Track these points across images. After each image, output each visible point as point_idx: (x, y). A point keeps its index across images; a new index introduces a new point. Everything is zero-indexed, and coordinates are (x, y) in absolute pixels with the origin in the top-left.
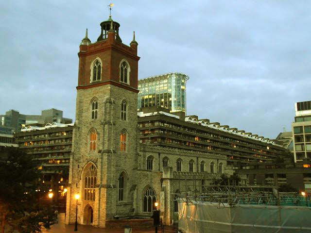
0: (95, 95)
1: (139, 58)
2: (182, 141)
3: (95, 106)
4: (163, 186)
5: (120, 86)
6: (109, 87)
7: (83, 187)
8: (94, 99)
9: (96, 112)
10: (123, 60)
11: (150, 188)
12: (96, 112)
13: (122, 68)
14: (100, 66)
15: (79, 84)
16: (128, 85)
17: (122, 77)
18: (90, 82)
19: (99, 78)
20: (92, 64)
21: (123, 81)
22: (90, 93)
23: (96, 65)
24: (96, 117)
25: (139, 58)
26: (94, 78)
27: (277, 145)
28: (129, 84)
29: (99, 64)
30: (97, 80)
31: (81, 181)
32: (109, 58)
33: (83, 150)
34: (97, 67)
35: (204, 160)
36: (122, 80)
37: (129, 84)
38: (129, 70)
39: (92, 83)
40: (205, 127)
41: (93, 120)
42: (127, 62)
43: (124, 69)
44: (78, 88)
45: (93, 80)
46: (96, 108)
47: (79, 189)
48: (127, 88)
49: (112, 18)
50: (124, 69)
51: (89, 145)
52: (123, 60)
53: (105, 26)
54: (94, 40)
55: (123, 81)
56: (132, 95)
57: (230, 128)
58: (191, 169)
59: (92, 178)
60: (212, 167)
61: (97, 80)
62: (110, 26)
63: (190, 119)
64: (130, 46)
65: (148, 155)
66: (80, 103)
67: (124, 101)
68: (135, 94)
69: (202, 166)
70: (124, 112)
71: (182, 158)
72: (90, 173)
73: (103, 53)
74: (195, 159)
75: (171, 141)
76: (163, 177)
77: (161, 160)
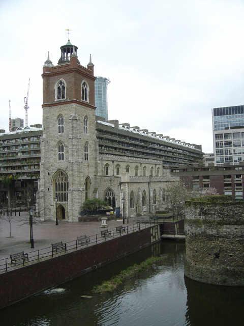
0: (60, 113)
2: (117, 148)
4: (121, 188)
7: (54, 191)
8: (60, 116)
9: (62, 127)
10: (83, 81)
11: (110, 190)
13: (83, 88)
14: (63, 87)
15: (43, 103)
17: (83, 96)
18: (56, 101)
19: (63, 97)
20: (56, 84)
22: (56, 111)
23: (59, 85)
24: (63, 132)
26: (59, 97)
27: (197, 149)
30: (61, 99)
32: (73, 80)
33: (52, 161)
35: (146, 165)
38: (88, 90)
40: (135, 134)
42: (87, 83)
52: (83, 81)
54: (55, 63)
56: (90, 112)
57: (149, 131)
58: (136, 174)
59: (62, 183)
60: (151, 171)
63: (123, 126)
64: (87, 67)
65: (105, 163)
67: (86, 117)
69: (144, 171)
70: (86, 127)
71: (130, 164)
72: (60, 179)
73: (67, 75)
74: (139, 165)
75: (107, 149)
76: (122, 181)
77: (114, 167)
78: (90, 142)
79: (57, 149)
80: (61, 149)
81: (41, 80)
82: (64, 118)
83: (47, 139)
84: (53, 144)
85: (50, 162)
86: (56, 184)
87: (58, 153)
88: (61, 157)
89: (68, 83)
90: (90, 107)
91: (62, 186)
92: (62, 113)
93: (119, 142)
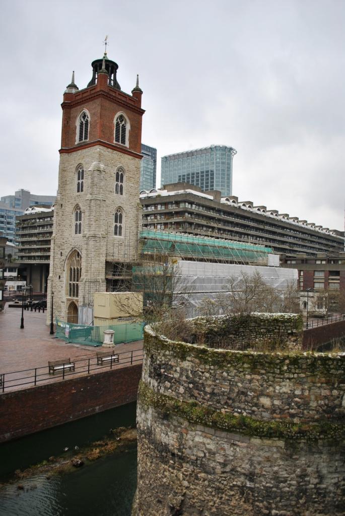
0: (80, 161)
1: (143, 112)
3: (81, 175)
5: (114, 148)
6: (98, 150)
7: (67, 280)
10: (119, 114)
12: (82, 182)
13: (118, 124)
14: (87, 121)
16: (126, 147)
18: (76, 143)
19: (86, 138)
20: (78, 118)
21: (119, 142)
22: (77, 157)
23: (82, 120)
25: (143, 112)
26: (81, 139)
28: (128, 147)
29: (86, 118)
30: (83, 140)
31: (65, 272)
32: (98, 109)
33: (66, 234)
34: (84, 122)
36: (117, 140)
37: (128, 147)
38: (128, 127)
39: (78, 144)
41: (79, 194)
43: (121, 125)
44: (61, 151)
45: (80, 140)
46: (82, 179)
47: (62, 283)
48: (124, 151)
49: (107, 55)
50: (121, 125)
51: (74, 228)
52: (119, 114)
53: (97, 65)
55: (119, 142)
56: (132, 162)
61: (83, 140)
62: (105, 68)
64: (131, 95)
66: (63, 171)
68: (137, 159)
72: (75, 262)
73: (91, 102)
78: (126, 208)
79: (74, 216)
80: (79, 216)
81: (60, 112)
82: (85, 170)
83: (61, 202)
84: (69, 208)
85: (64, 236)
86: (71, 269)
87: (74, 222)
88: (78, 229)
89: (93, 115)
90: (130, 153)
91: (74, 271)
92: (82, 162)
93: (219, 220)
